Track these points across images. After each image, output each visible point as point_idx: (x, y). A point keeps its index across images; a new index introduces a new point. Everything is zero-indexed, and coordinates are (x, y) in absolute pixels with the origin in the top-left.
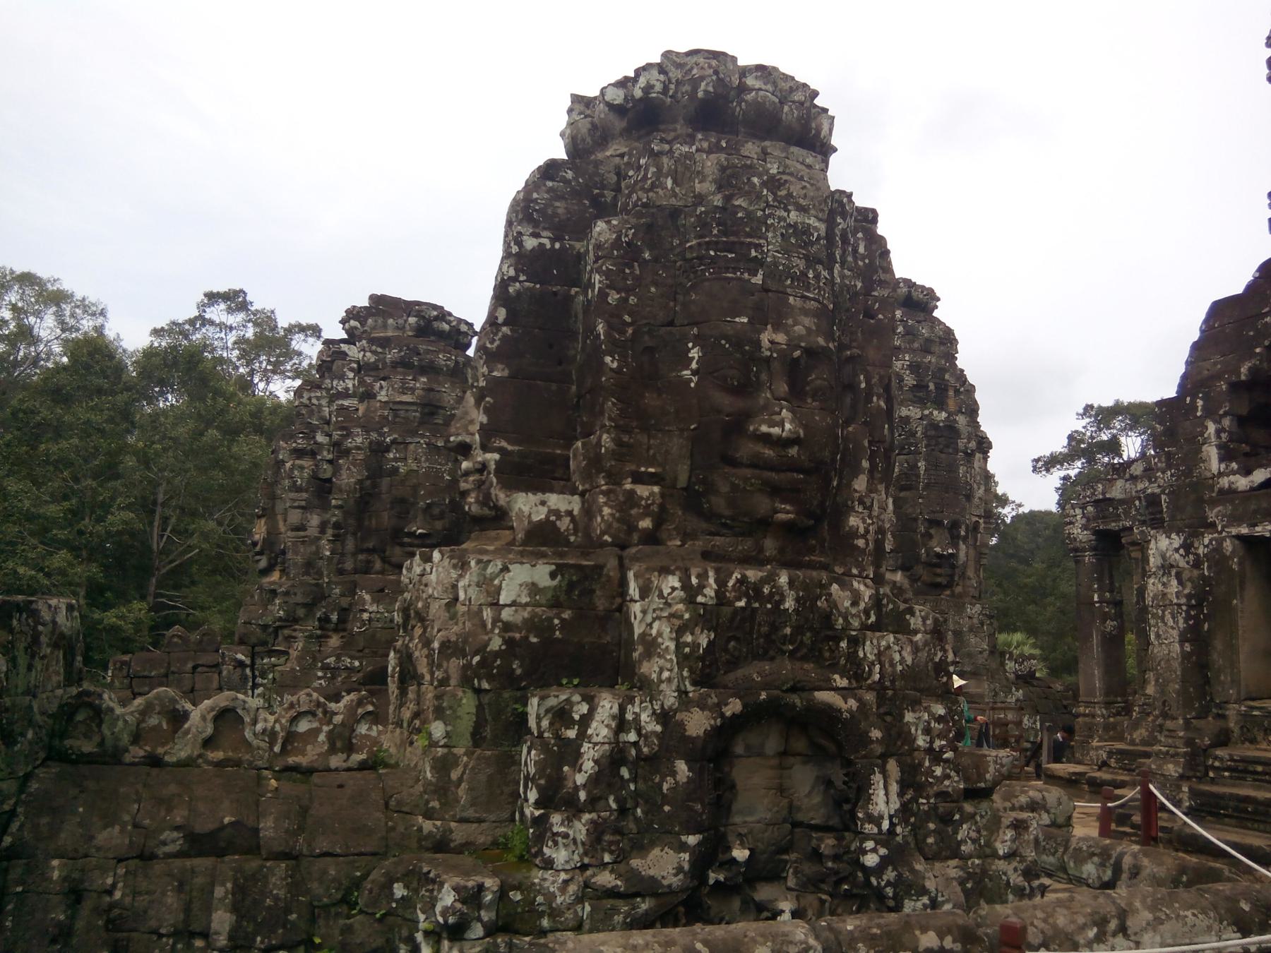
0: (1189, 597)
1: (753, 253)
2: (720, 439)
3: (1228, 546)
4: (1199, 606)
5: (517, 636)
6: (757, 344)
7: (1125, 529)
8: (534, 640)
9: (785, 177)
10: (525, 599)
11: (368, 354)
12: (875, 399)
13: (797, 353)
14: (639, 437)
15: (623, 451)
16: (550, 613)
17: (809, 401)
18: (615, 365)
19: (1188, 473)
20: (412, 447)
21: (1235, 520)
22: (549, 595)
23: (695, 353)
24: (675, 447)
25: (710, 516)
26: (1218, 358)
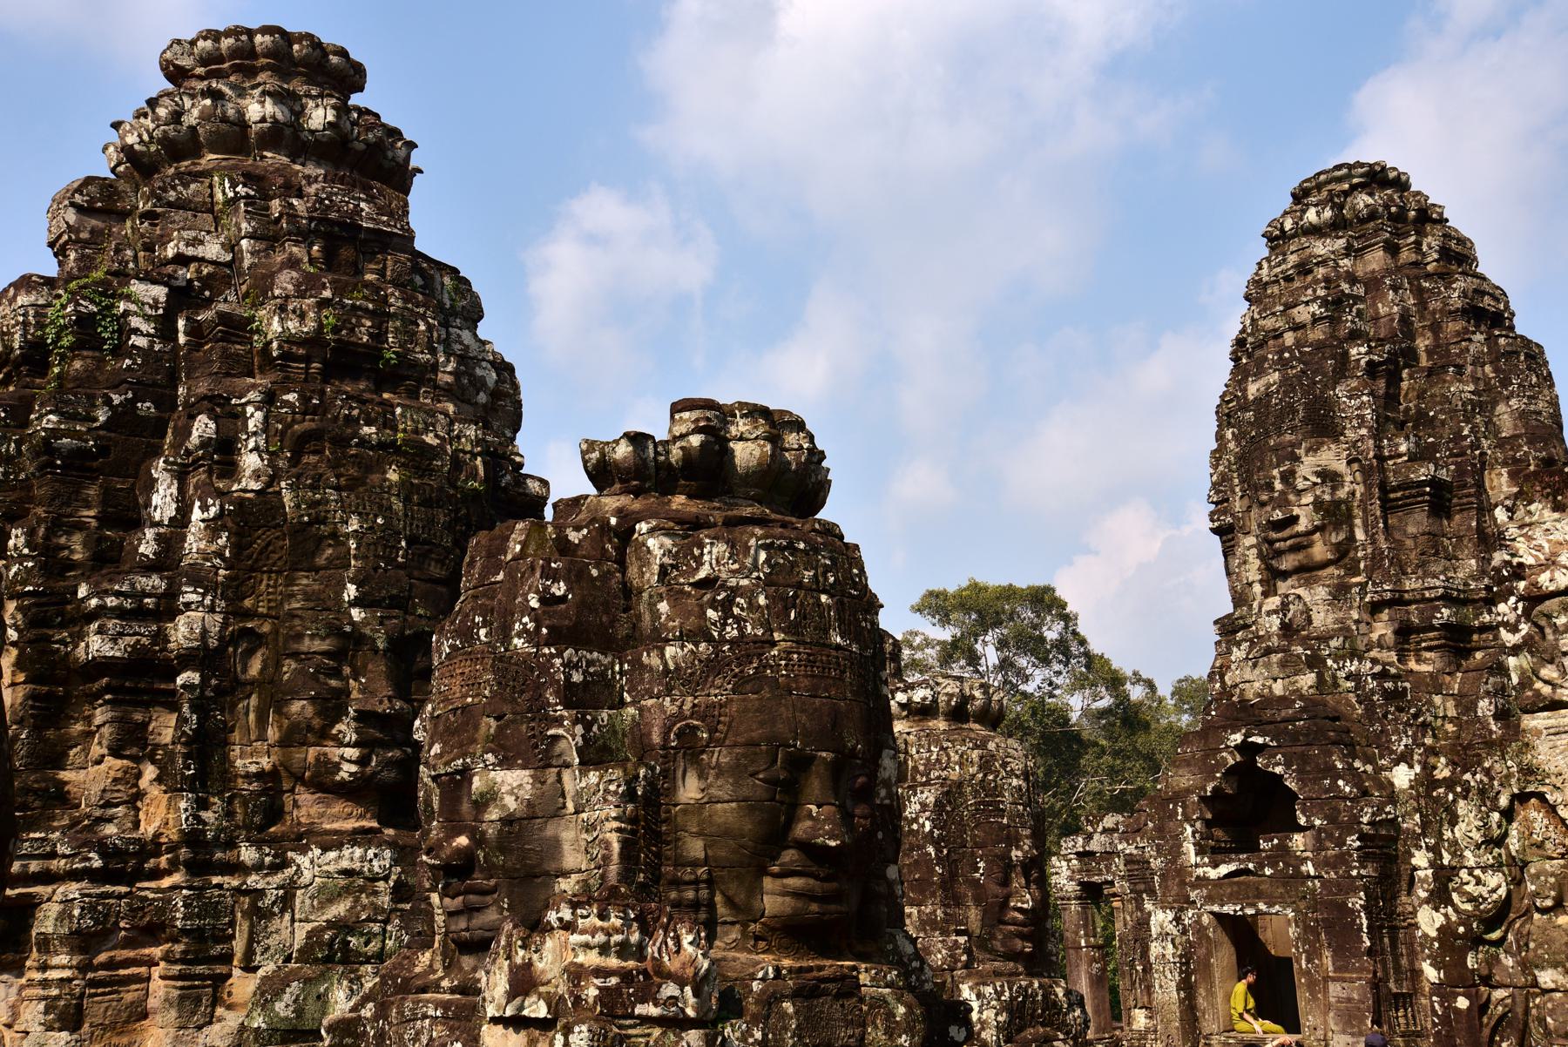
0: (1181, 956)
2: (996, 912)
3: (1206, 919)
4: (1187, 963)
7: (1107, 882)
15: (948, 918)
19: (1174, 861)
21: (1210, 899)
23: (981, 865)
24: (974, 915)
25: (992, 951)
26: (1188, 776)
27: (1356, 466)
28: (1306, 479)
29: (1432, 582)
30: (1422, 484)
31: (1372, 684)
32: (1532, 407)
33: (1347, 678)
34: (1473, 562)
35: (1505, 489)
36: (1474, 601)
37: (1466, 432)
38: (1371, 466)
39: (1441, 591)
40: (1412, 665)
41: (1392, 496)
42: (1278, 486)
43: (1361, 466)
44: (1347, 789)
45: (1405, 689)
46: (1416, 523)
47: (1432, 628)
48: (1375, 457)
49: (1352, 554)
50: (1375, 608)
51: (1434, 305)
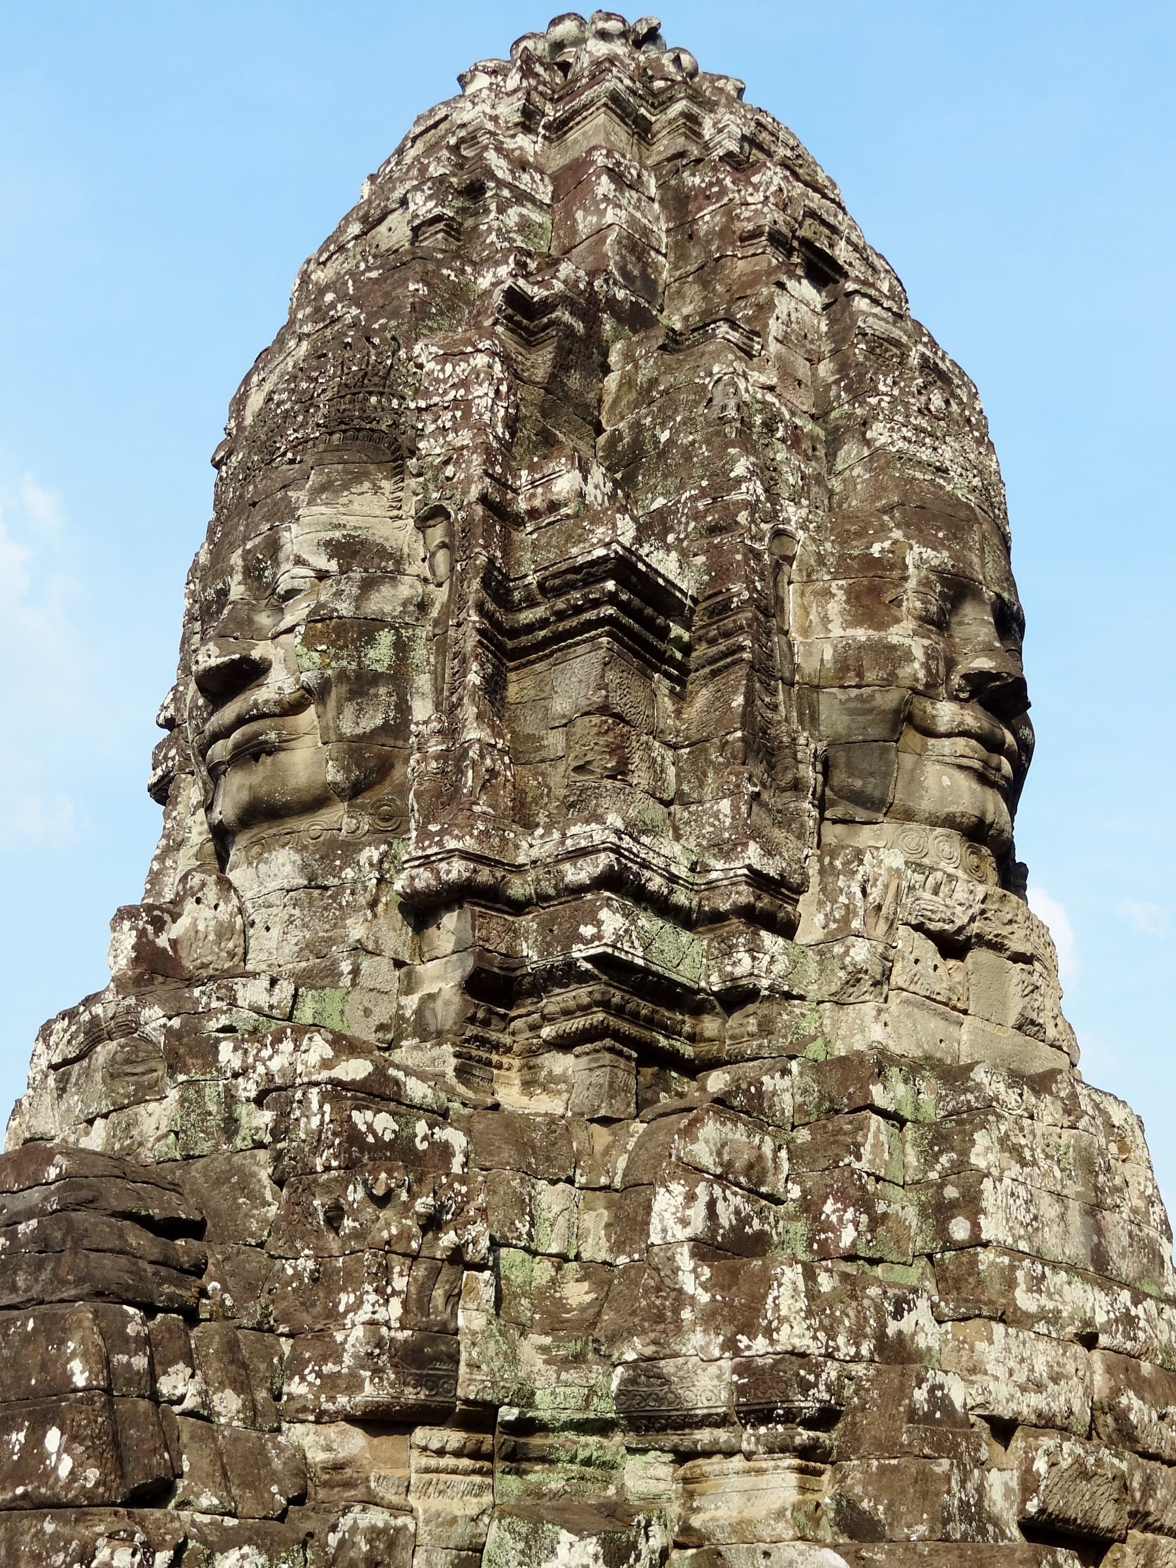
27: (437, 533)
28: (299, 561)
29: (581, 833)
30: (592, 572)
31: (315, 1116)
32: (925, 455)
33: (259, 1101)
34: (725, 805)
35: (836, 631)
36: (716, 918)
37: (740, 470)
38: (468, 522)
39: (604, 860)
40: (510, 1094)
41: (527, 616)
42: (237, 591)
43: (450, 533)
44: (65, 1466)
45: (444, 1151)
46: (575, 680)
47: (569, 974)
48: (484, 499)
49: (397, 773)
50: (421, 911)
51: (708, 219)
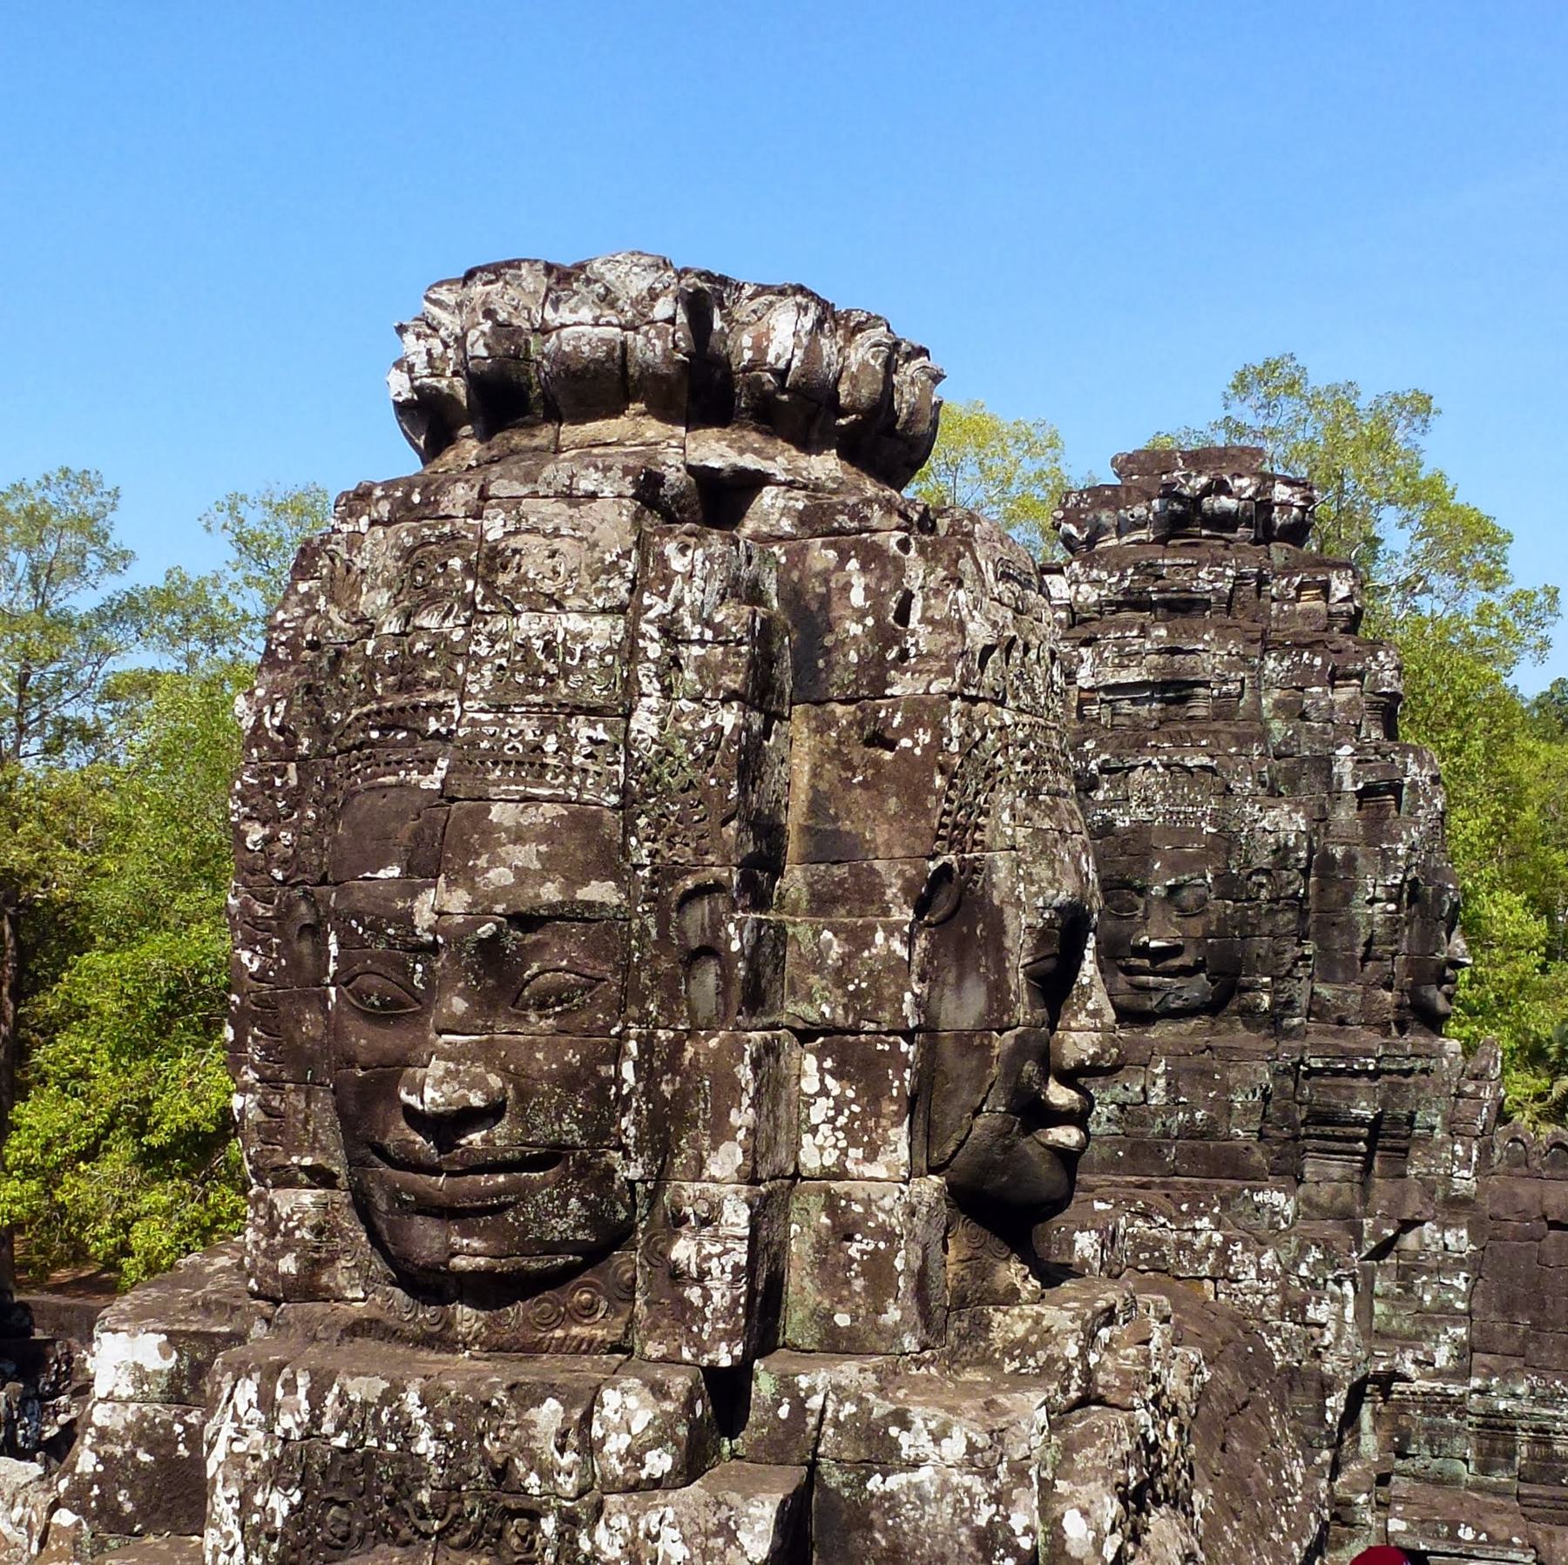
1: (433, 725)
5: (119, 1451)
6: (407, 918)
8: (144, 1457)
9: (514, 543)
10: (125, 1391)
11: (1084, 588)
12: (880, 937)
13: (486, 930)
14: (292, 1096)
16: (166, 1414)
17: (533, 1018)
18: (254, 967)
20: (1135, 775)
22: (163, 1381)
